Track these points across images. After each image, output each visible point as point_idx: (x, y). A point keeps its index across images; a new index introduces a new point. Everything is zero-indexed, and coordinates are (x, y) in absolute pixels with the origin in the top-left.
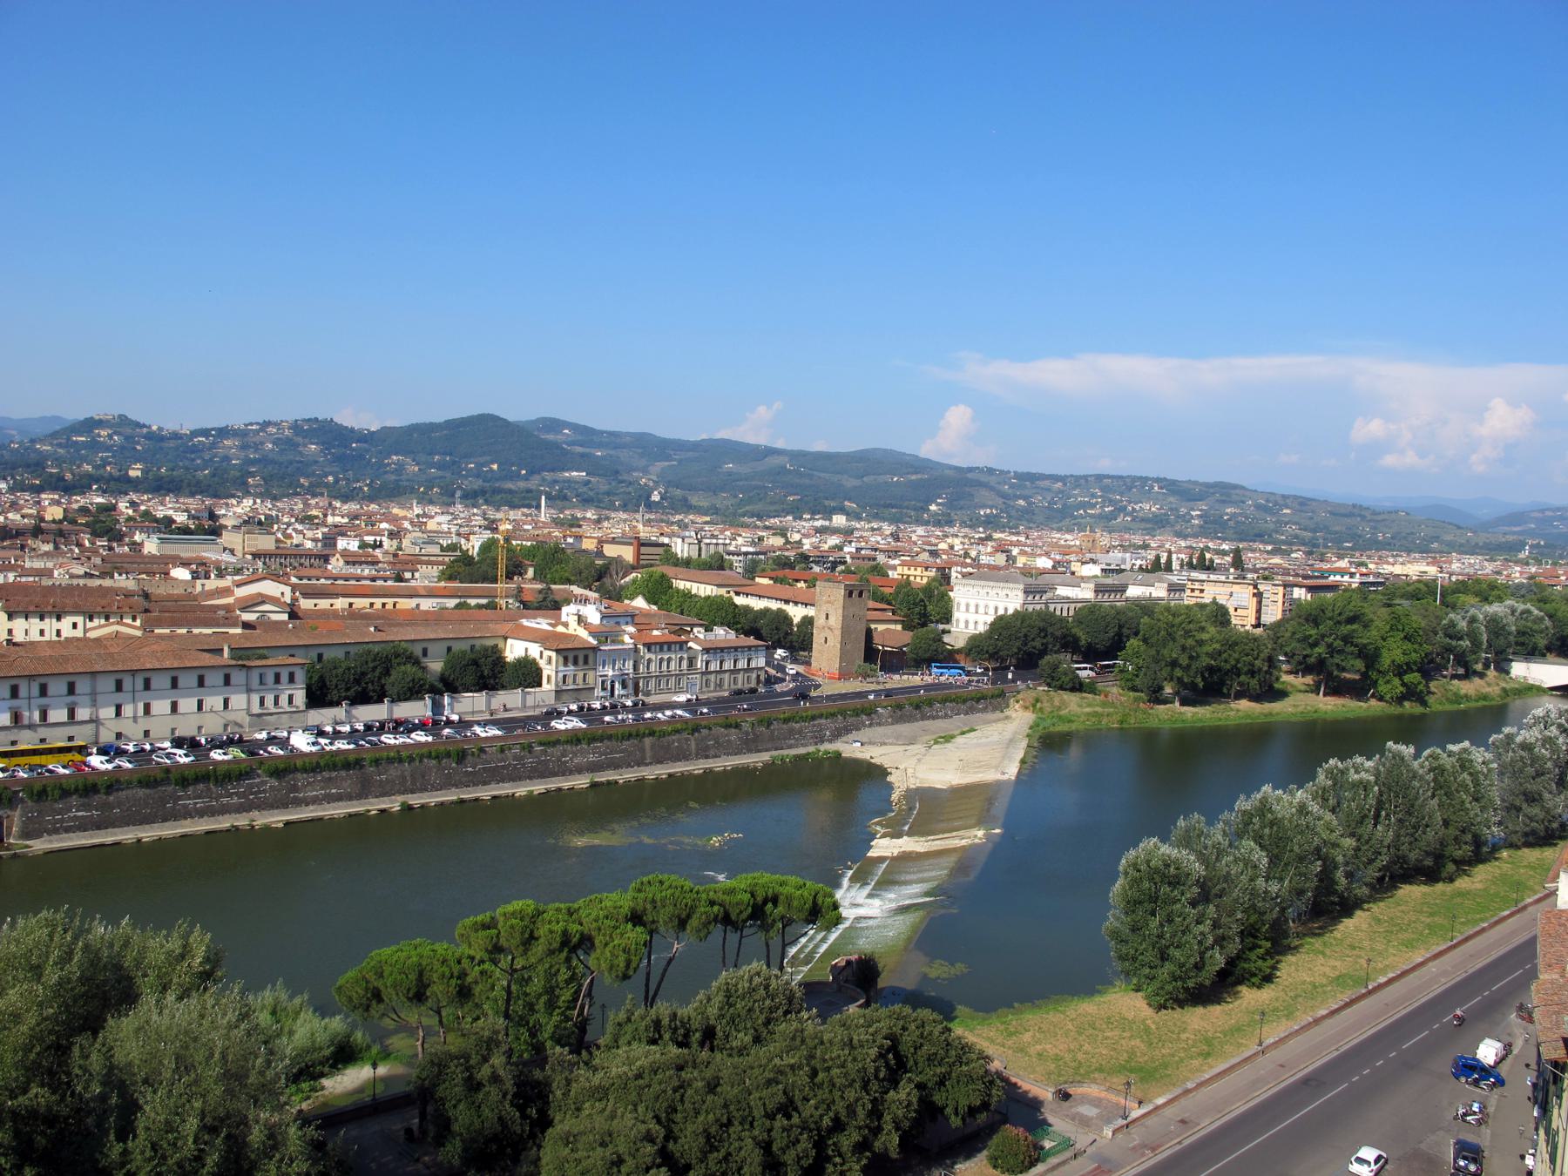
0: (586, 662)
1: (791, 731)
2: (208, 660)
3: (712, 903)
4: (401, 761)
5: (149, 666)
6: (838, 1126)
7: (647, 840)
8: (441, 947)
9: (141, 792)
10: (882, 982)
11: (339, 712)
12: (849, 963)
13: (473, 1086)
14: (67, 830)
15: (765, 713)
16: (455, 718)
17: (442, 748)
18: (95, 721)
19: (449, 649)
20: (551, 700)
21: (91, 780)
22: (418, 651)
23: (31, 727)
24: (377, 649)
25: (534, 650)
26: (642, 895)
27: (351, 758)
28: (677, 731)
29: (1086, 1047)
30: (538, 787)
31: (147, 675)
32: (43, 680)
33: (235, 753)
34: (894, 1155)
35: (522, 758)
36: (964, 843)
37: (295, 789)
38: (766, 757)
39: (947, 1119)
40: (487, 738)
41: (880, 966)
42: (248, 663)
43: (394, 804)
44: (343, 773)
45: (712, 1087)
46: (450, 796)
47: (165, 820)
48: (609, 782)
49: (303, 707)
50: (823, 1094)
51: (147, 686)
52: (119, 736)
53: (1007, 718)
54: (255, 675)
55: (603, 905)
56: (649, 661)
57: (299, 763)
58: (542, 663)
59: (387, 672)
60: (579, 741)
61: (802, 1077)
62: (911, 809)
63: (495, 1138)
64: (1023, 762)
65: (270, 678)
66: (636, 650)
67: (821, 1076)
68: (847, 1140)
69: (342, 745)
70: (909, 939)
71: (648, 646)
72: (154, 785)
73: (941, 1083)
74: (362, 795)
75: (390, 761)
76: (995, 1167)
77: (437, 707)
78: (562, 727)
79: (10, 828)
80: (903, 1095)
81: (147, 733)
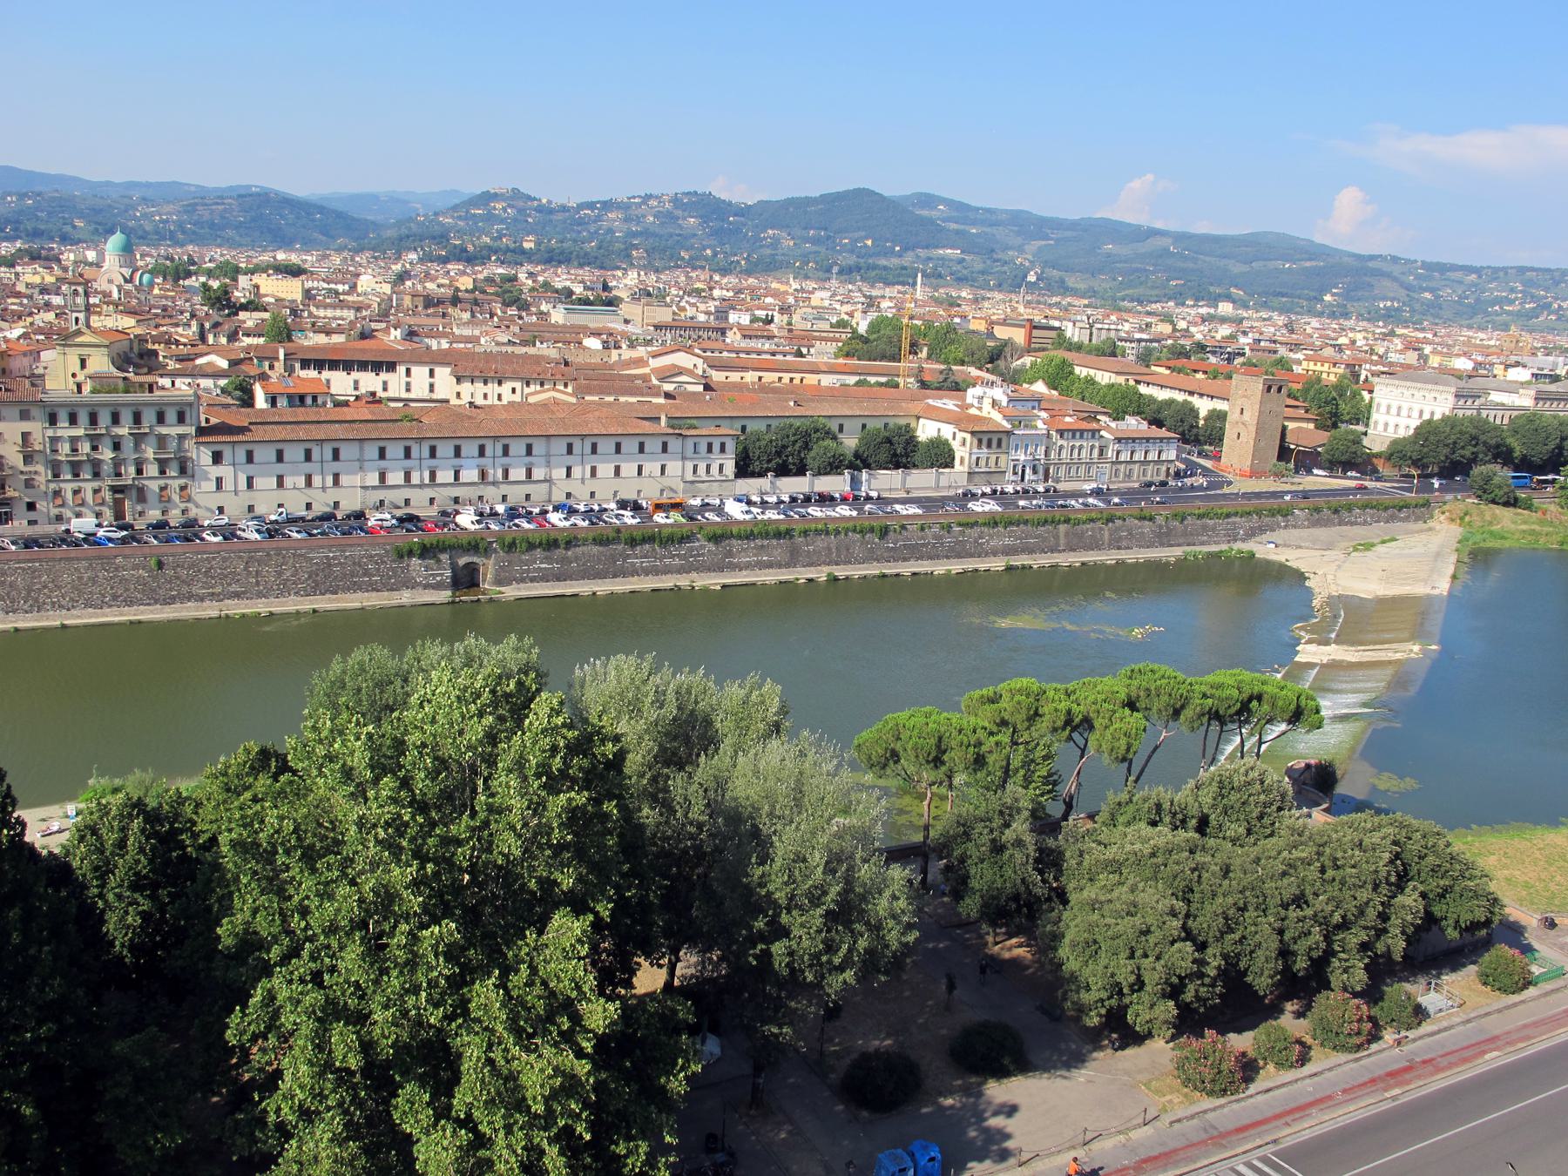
0: (999, 445)
1: (1205, 527)
2: (648, 427)
3: (1205, 696)
4: (828, 533)
6: (1345, 925)
7: (1069, 627)
8: (955, 718)
9: (596, 549)
10: (1340, 789)
11: (764, 483)
12: (1308, 766)
13: (998, 848)
14: (533, 580)
15: (1179, 507)
16: (874, 494)
18: (548, 480)
19: (864, 426)
20: (963, 481)
21: (553, 535)
22: (835, 428)
23: (494, 483)
24: (797, 423)
25: (947, 431)
26: (1135, 683)
27: (783, 528)
28: (1092, 520)
29: (1558, 878)
30: (956, 567)
31: (594, 440)
32: (506, 441)
33: (676, 517)
34: (1398, 957)
35: (941, 537)
36: (1398, 656)
37: (730, 554)
38: (1178, 552)
39: (1442, 930)
40: (908, 516)
41: (1339, 773)
42: (681, 431)
43: (821, 574)
44: (774, 542)
45: (1226, 871)
46: (873, 570)
47: (615, 576)
48: (1024, 567)
49: (732, 477)
50: (1333, 890)
51: (594, 450)
52: (569, 495)
53: (1430, 529)
54: (690, 443)
55: (1097, 691)
56: (1061, 447)
57: (735, 531)
58: (955, 445)
59: (807, 447)
60: (996, 524)
61: (1312, 873)
62: (1336, 617)
63: (1016, 897)
64: (1454, 577)
65: (703, 448)
66: (1048, 436)
67: (1330, 873)
68: (1355, 937)
69: (772, 515)
70: (1352, 749)
71: (1061, 433)
72: (612, 543)
73: (1442, 896)
74: (791, 563)
75: (818, 532)
76: (1485, 984)
77: (855, 483)
78: (979, 509)
79: (485, 575)
80: (1409, 900)
81: (592, 494)
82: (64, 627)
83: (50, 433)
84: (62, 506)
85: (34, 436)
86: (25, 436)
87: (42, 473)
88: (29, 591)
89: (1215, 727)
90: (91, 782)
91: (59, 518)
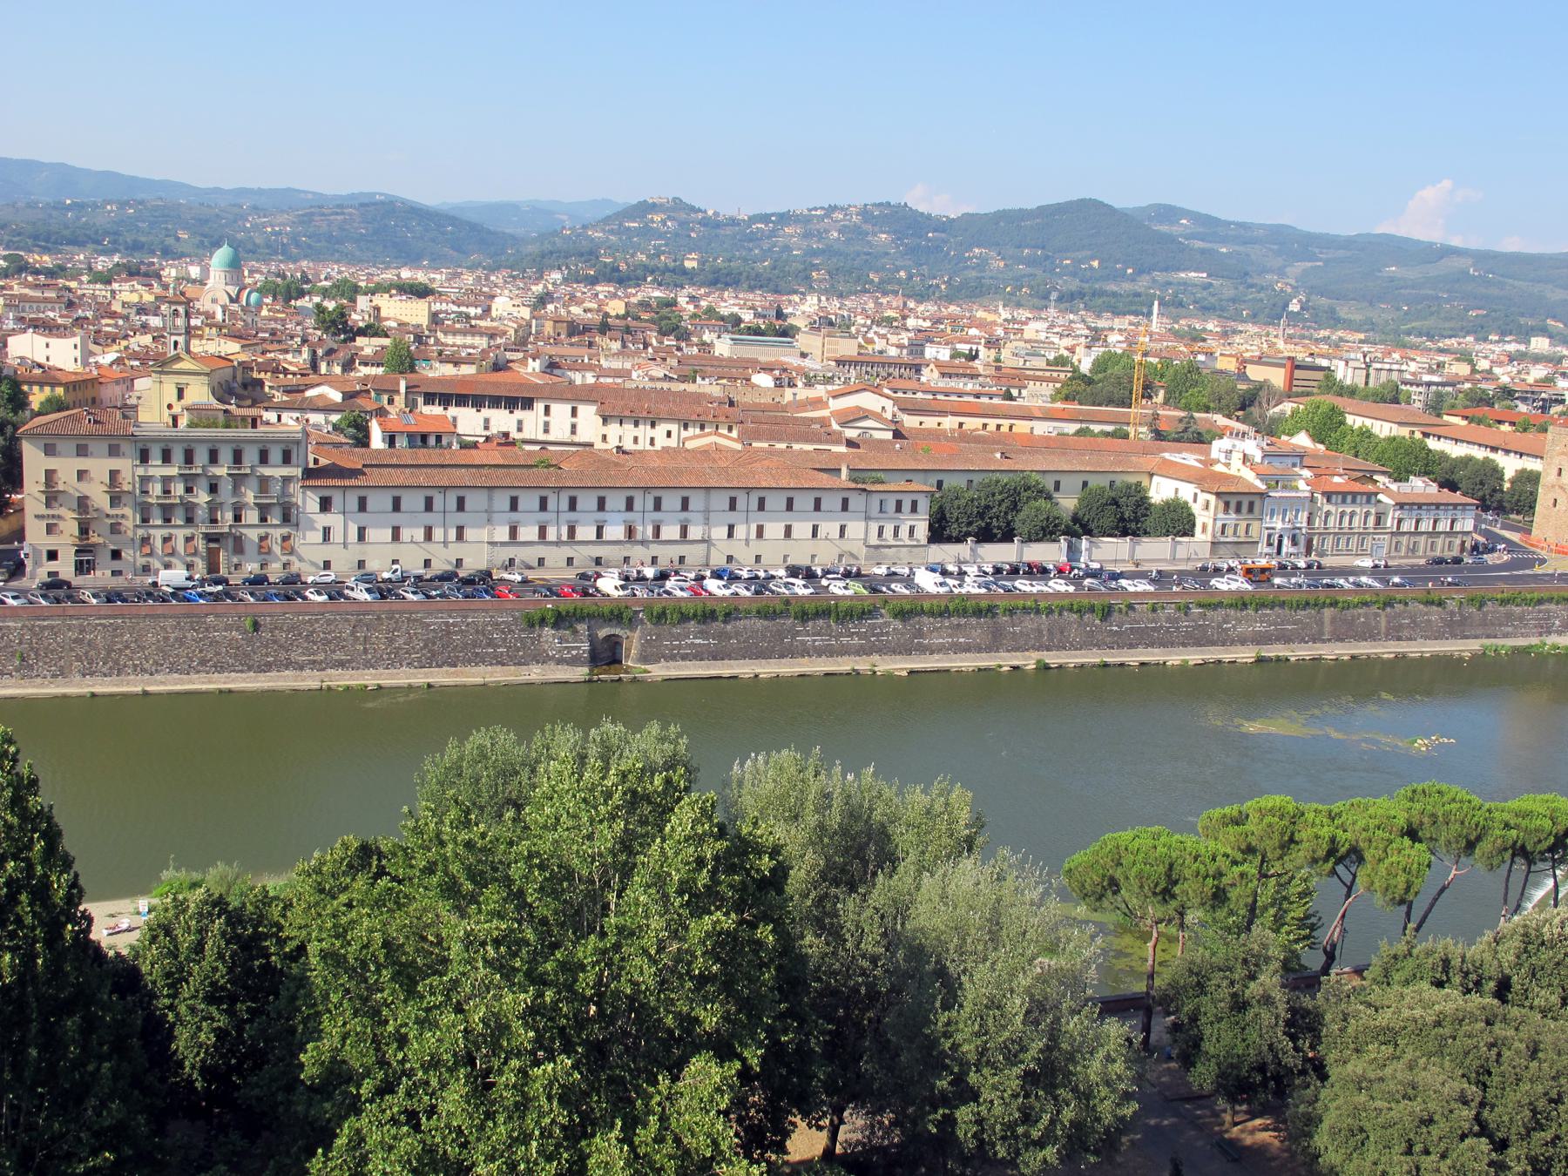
0: (1251, 510)
1: (1509, 616)
2: (825, 480)
3: (1507, 826)
4: (1038, 612)
5: (764, 484)
7: (1334, 735)
8: (1190, 841)
9: (760, 624)
11: (963, 550)
13: (1239, 1005)
14: (684, 658)
15: (1478, 590)
17: (1085, 601)
19: (1085, 484)
20: (1205, 552)
21: (709, 606)
22: (1050, 487)
23: (643, 543)
24: (1005, 479)
25: (1187, 492)
26: (1418, 806)
27: (984, 604)
28: (1365, 604)
30: (1194, 656)
31: (762, 494)
32: (657, 493)
33: (856, 588)
35: (1177, 620)
38: (1474, 645)
40: (1136, 594)
42: (863, 486)
44: (973, 621)
45: (1534, 1052)
46: (1092, 657)
47: (782, 656)
48: (1278, 659)
49: (924, 541)
51: (761, 506)
52: (730, 559)
55: (1368, 814)
56: (1328, 514)
57: (926, 605)
58: (1196, 509)
59: (1015, 507)
60: (1245, 606)
63: (1262, 1068)
65: (891, 506)
66: (1312, 499)
71: (1328, 496)
72: (778, 615)
74: (992, 647)
75: (1026, 610)
77: (1073, 552)
78: (1224, 587)
79: (629, 650)
81: (758, 558)
82: (145, 693)
83: (141, 471)
84: (150, 555)
85: (123, 474)
86: (114, 474)
87: (129, 516)
88: (110, 651)
89: (1520, 865)
90: (166, 875)
91: (146, 569)
